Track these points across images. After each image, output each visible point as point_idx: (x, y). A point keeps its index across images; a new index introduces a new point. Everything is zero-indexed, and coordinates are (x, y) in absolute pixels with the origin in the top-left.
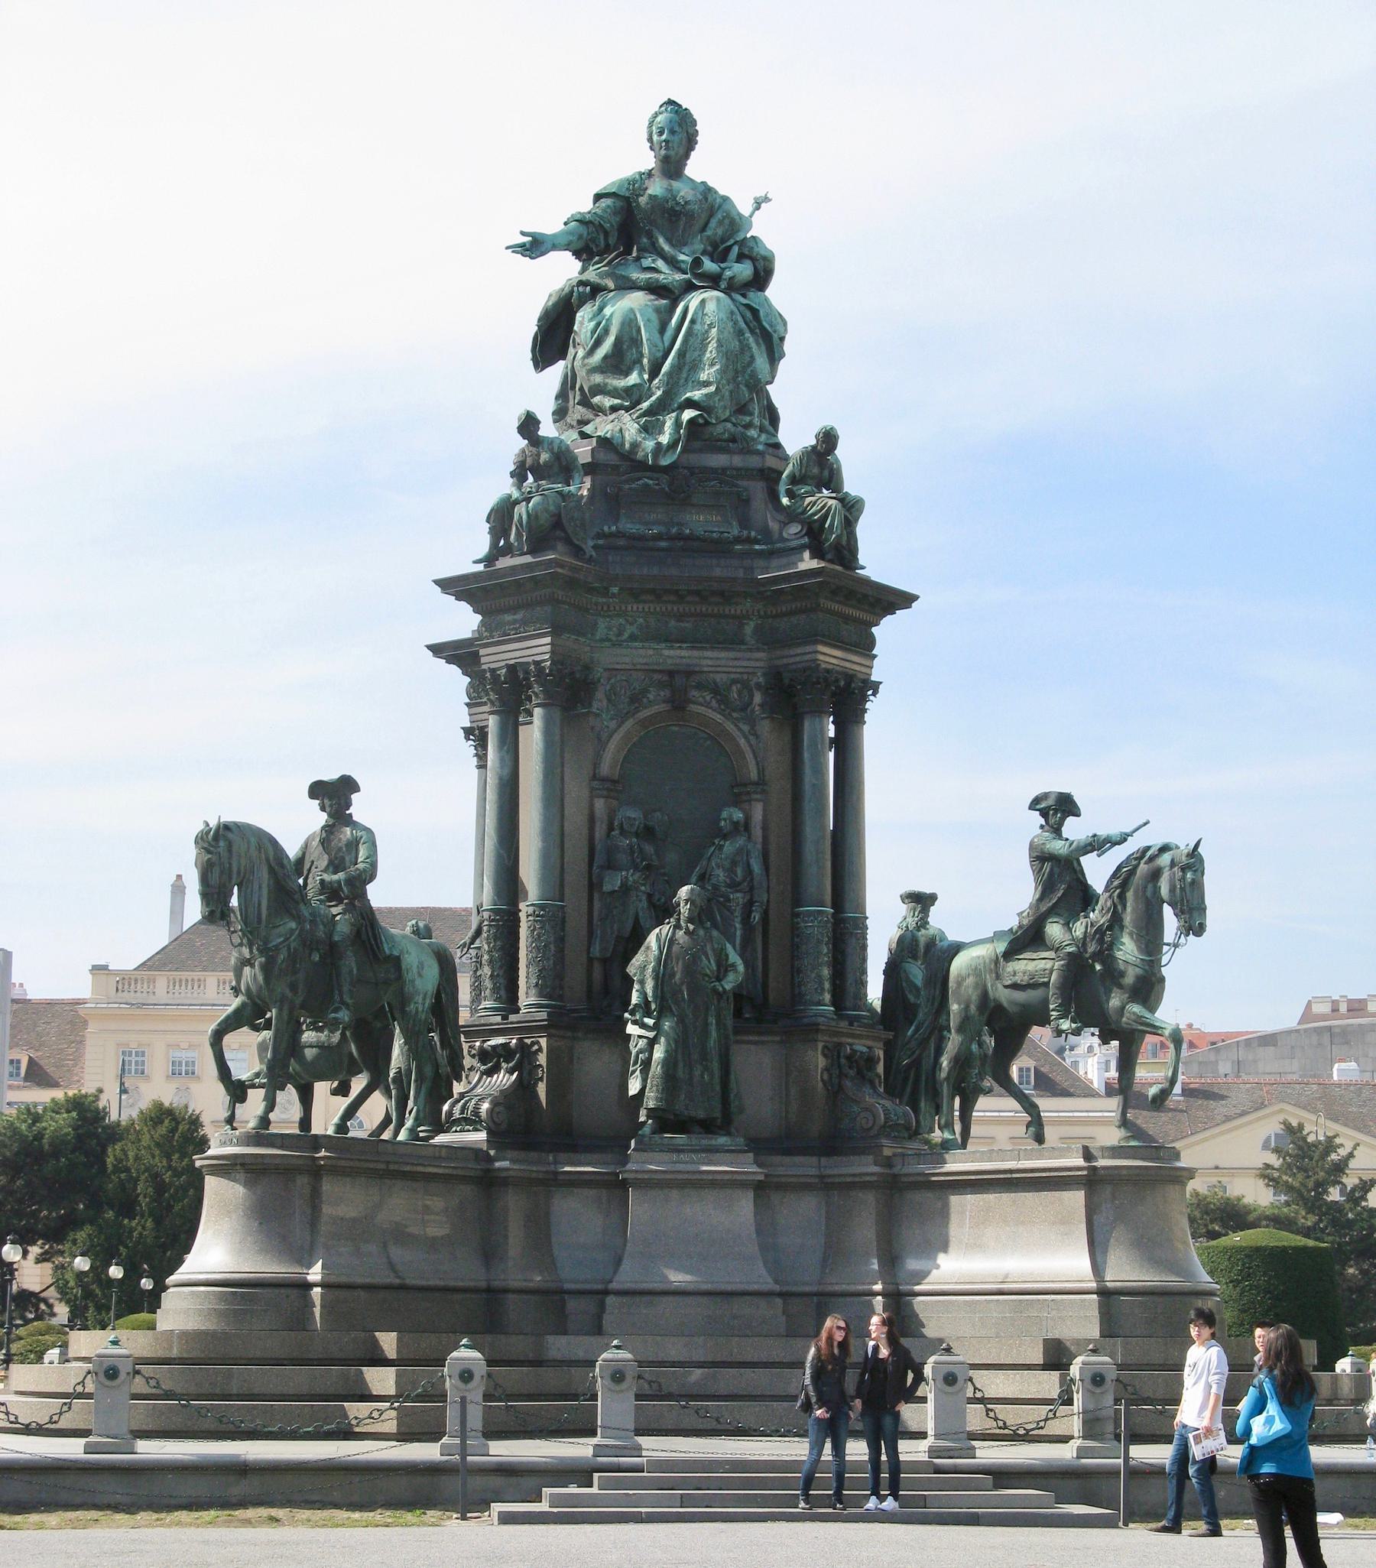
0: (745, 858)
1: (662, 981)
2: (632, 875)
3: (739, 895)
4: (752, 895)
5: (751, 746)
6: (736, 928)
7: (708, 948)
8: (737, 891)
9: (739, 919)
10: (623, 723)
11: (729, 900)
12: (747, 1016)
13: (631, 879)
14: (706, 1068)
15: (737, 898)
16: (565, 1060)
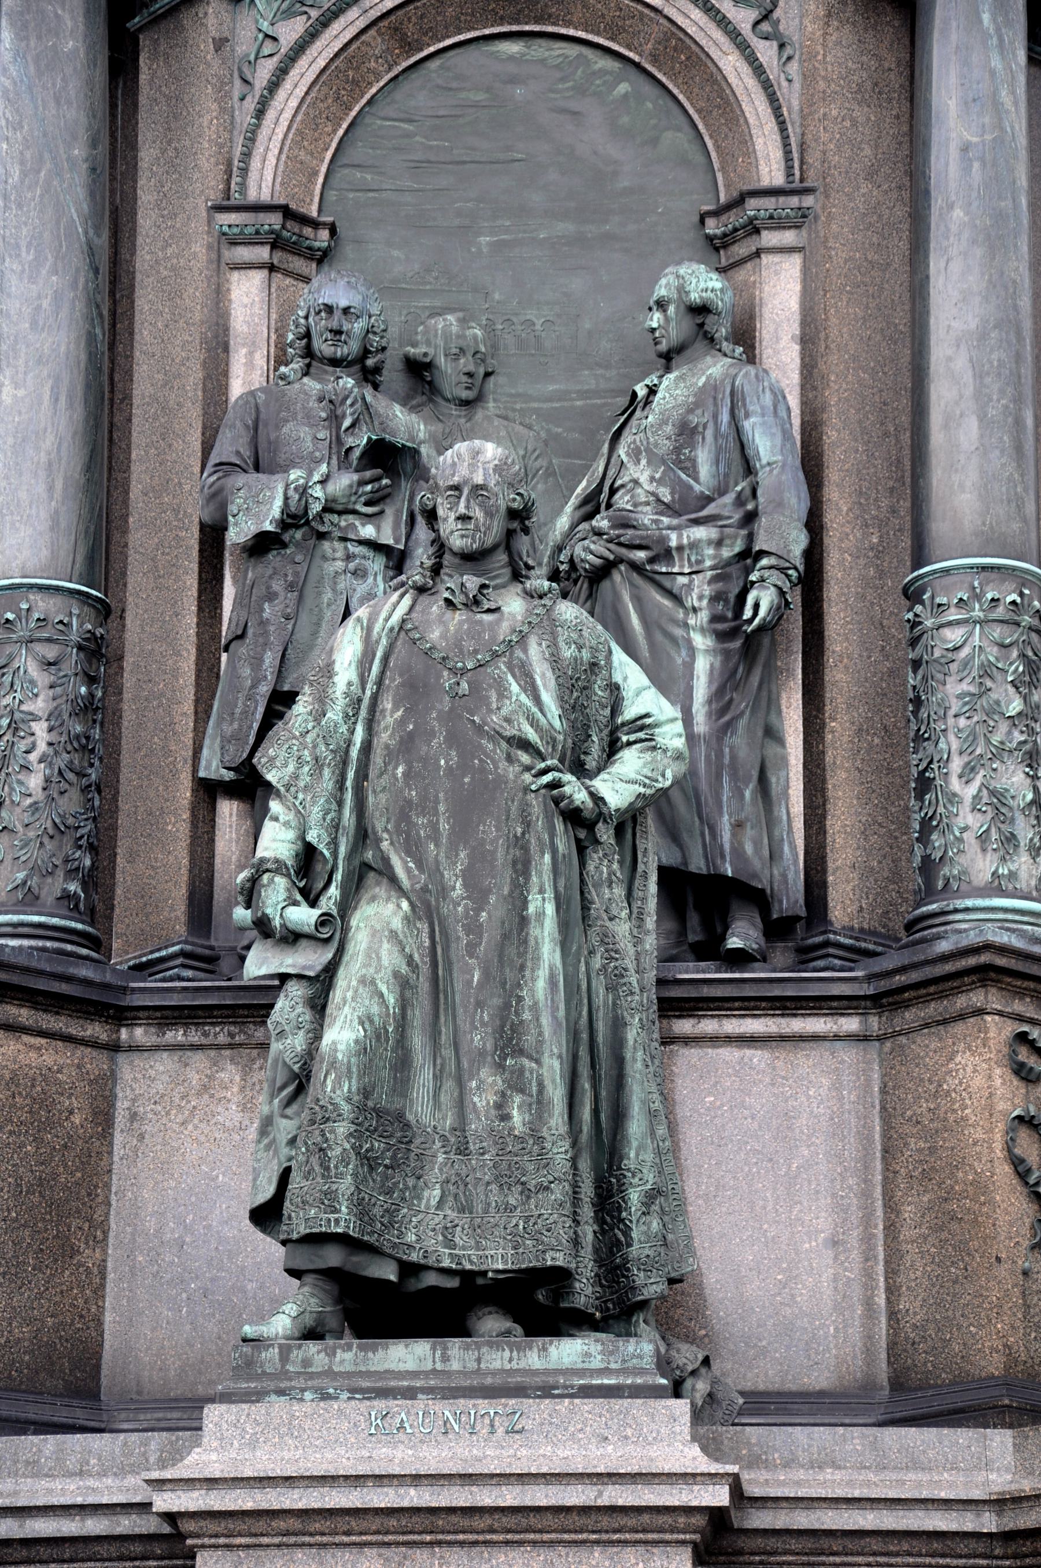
0: (725, 417)
1: (362, 775)
2: (323, 482)
3: (700, 533)
4: (750, 538)
5: (758, 70)
6: (692, 651)
7: (535, 652)
8: (697, 522)
9: (704, 616)
10: (324, 23)
11: (667, 554)
12: (734, 942)
13: (318, 492)
14: (517, 1083)
15: (694, 545)
16: (77, 1119)
